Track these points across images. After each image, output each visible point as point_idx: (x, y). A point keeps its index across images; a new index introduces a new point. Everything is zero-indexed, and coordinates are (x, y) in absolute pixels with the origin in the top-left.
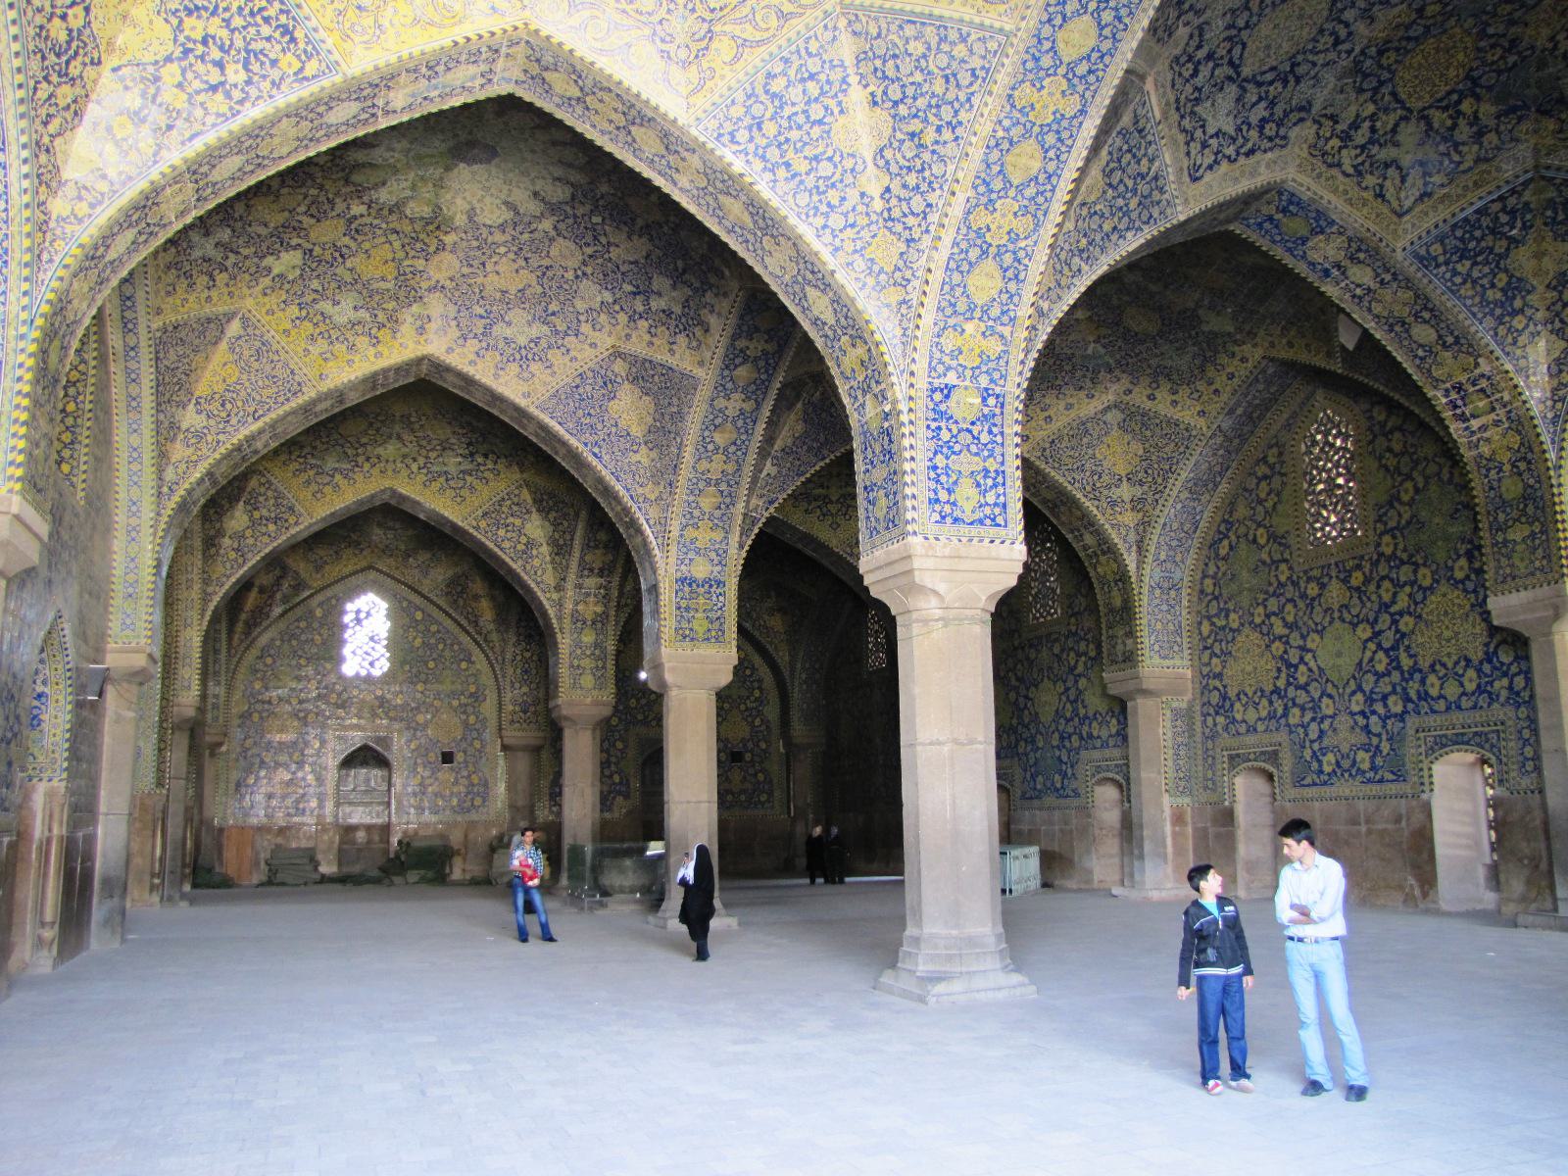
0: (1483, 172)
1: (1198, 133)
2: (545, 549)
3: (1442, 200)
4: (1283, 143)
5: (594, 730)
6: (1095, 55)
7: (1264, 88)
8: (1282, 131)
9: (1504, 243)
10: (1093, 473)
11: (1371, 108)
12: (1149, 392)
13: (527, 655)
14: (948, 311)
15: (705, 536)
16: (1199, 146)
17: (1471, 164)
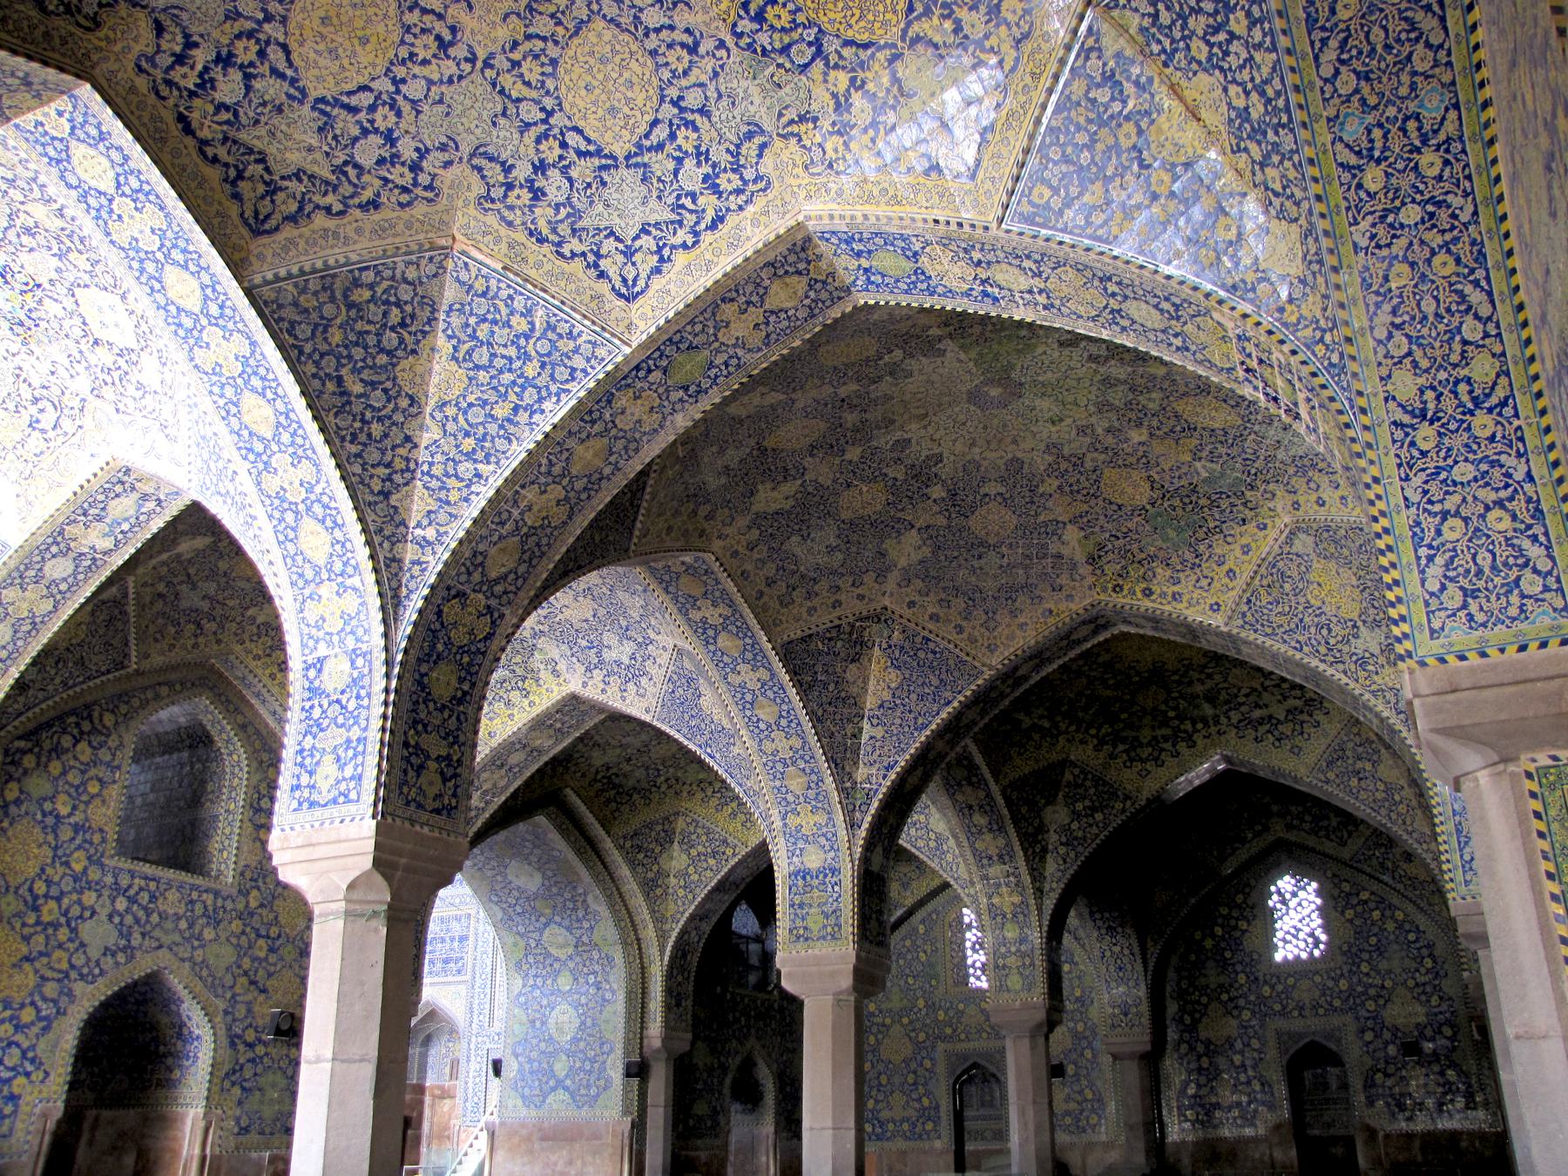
0: (1033, 53)
1: (609, 245)
2: (952, 842)
3: (1008, 124)
4: (762, 185)
5: (1033, 1037)
6: (209, 291)
7: (669, 148)
8: (749, 174)
9: (1129, 127)
10: (1319, 627)
11: (841, 79)
12: (1313, 497)
13: (1117, 949)
14: (301, 583)
15: (808, 821)
16: (620, 259)
17: (1013, 53)
